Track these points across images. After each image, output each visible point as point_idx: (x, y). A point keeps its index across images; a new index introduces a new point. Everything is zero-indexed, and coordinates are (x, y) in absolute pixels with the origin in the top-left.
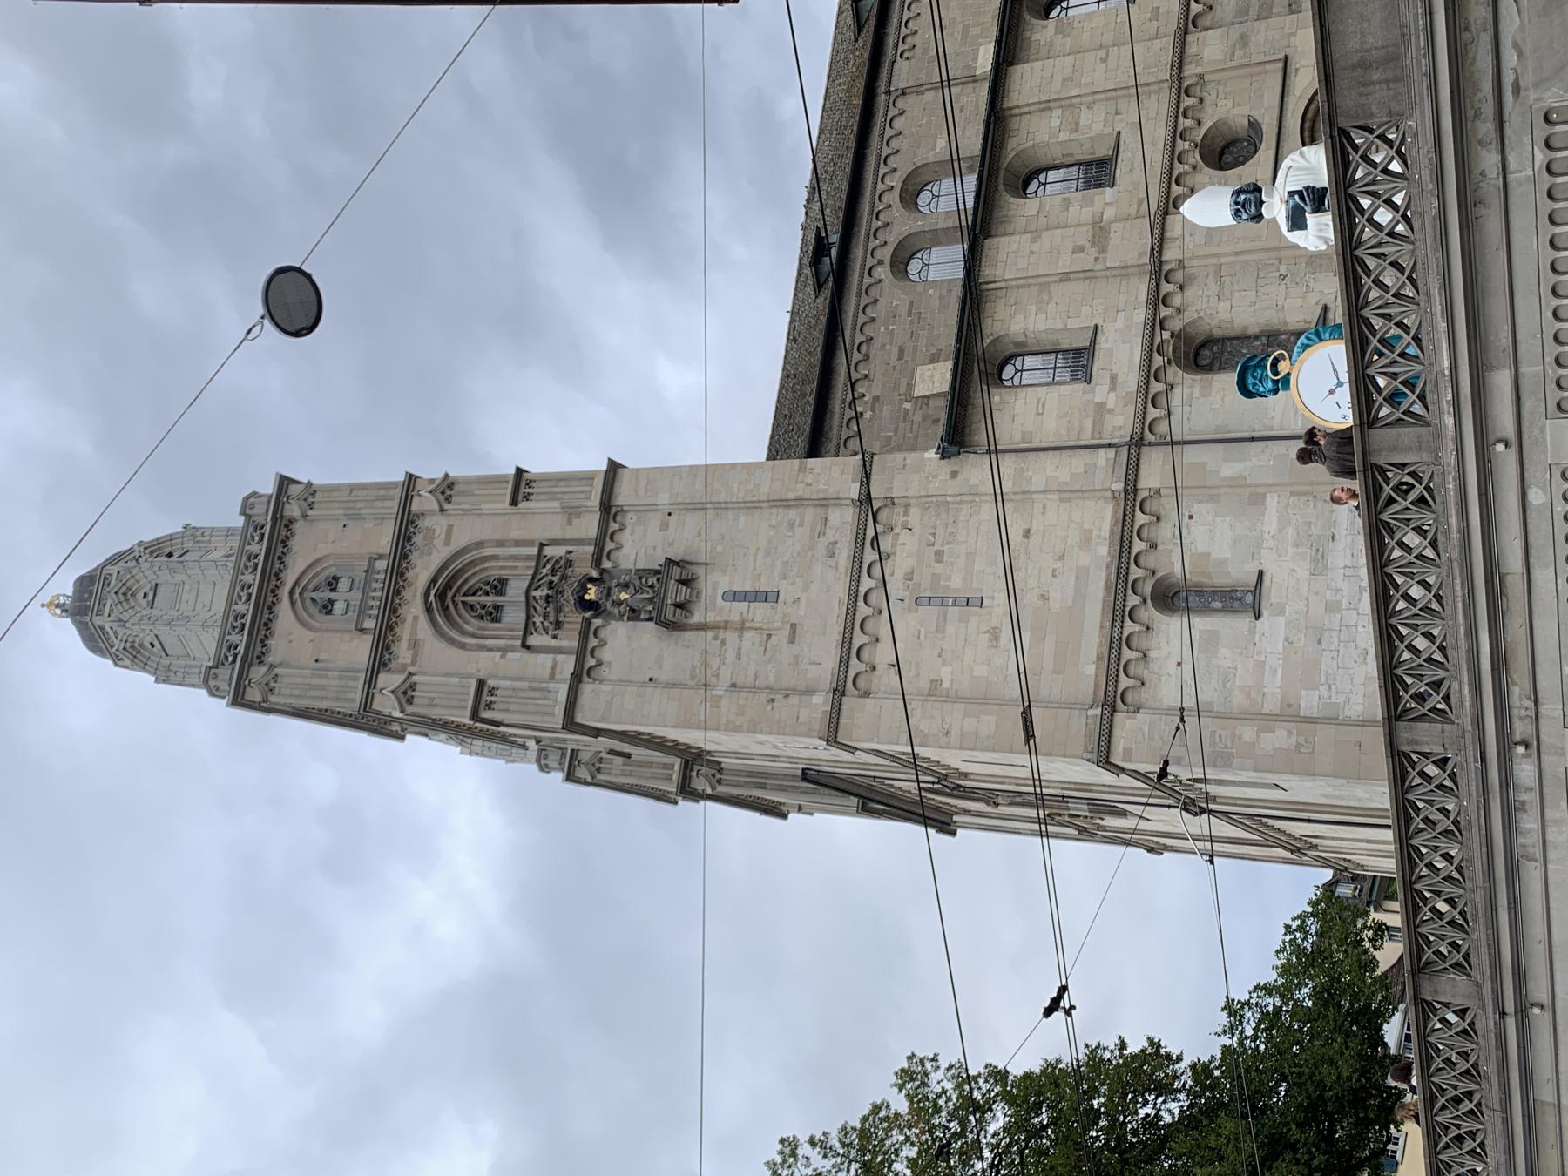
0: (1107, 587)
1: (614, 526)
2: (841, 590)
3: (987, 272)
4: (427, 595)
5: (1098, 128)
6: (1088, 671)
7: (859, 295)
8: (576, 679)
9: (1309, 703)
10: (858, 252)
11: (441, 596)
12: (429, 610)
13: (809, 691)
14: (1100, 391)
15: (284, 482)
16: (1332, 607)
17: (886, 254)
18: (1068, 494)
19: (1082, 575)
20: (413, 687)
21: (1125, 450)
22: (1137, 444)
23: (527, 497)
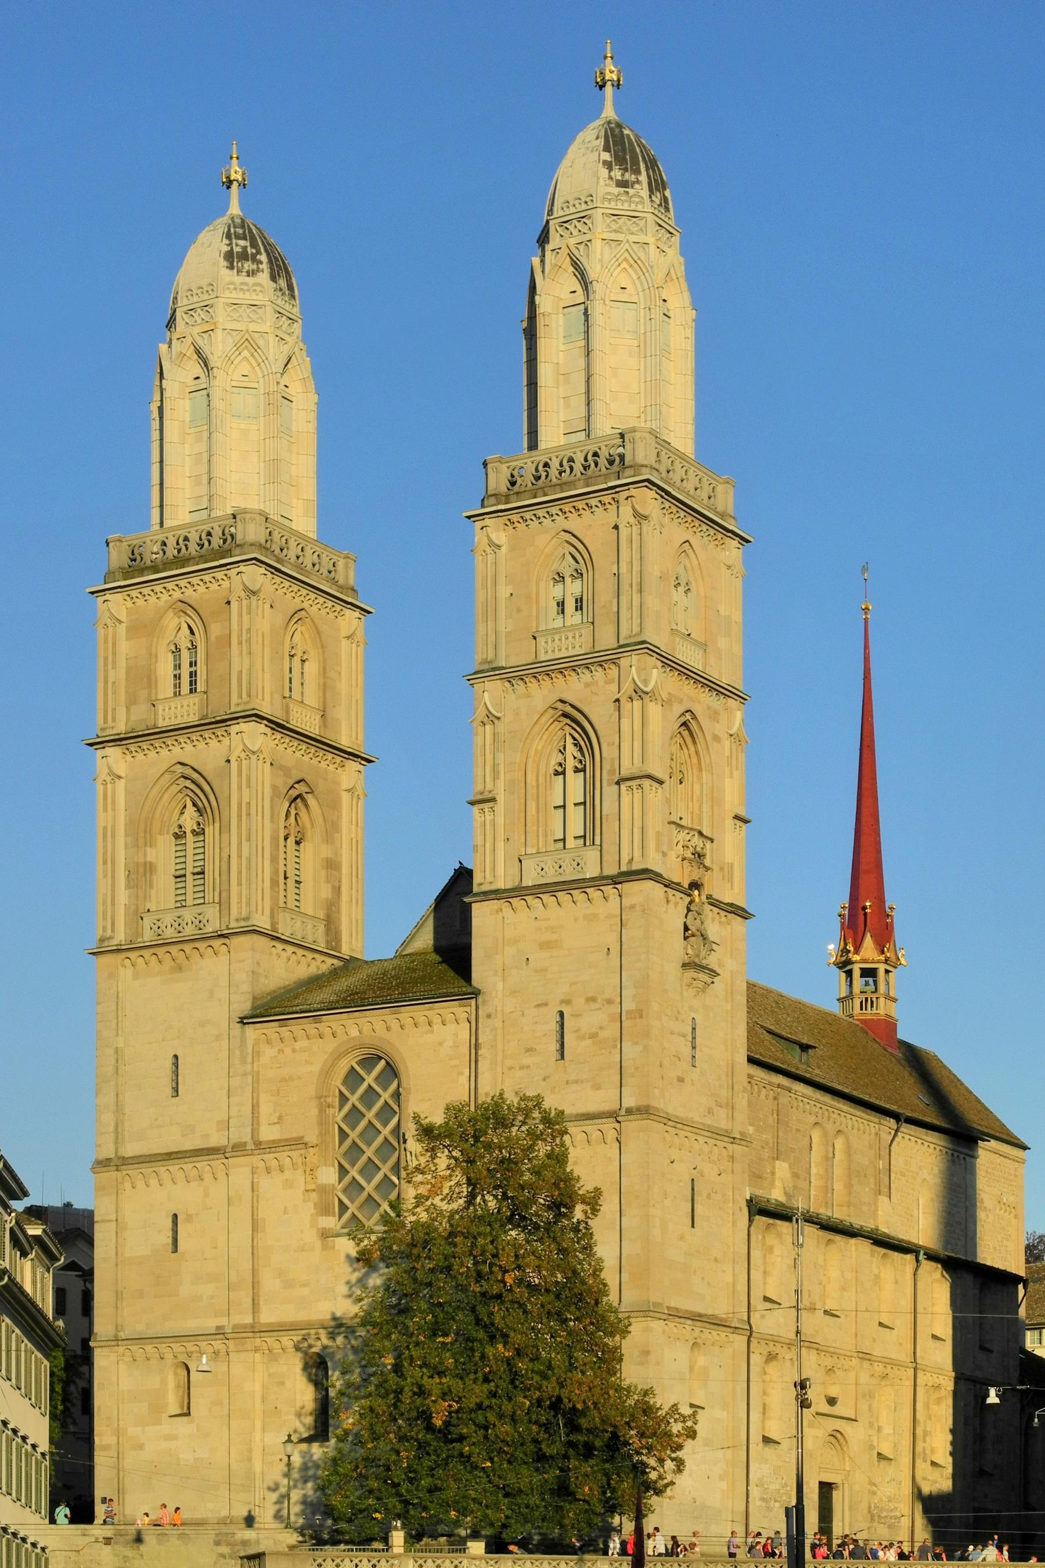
1: (723, 913)
8: (668, 885)
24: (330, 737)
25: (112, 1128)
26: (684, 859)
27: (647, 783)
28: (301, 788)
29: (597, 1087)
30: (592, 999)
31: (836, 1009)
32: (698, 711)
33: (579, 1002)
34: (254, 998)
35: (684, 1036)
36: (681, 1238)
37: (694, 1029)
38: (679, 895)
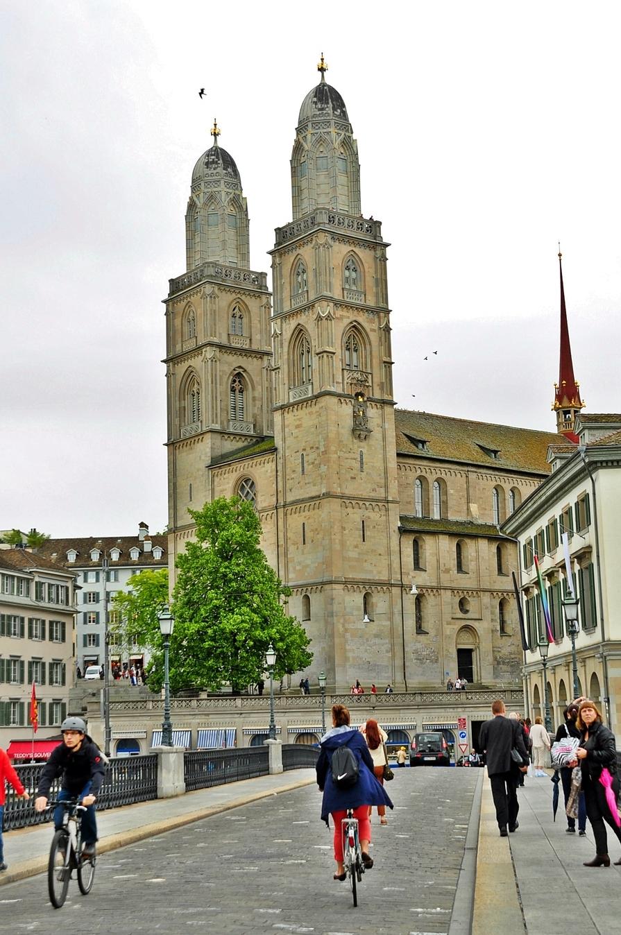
0: (369, 580)
1: (378, 405)
2: (365, 495)
3: (441, 537)
4: (356, 321)
5: (471, 567)
6: (351, 576)
7: (414, 464)
8: (339, 396)
9: (348, 635)
10: (425, 463)
11: (354, 326)
12: (351, 323)
13: (340, 486)
14: (412, 573)
15: (387, 245)
16: (367, 640)
17: (424, 474)
18: (390, 566)
19: (371, 572)
20: (331, 320)
21: (400, 583)
22: (402, 586)
23: (385, 366)
24: (255, 347)
25: (173, 516)
26: (351, 384)
27: (325, 355)
28: (241, 370)
29: (314, 485)
30: (312, 448)
31: (554, 430)
32: (360, 320)
33: (308, 449)
34: (212, 458)
35: (355, 459)
36: (356, 547)
37: (361, 456)
38: (348, 400)
